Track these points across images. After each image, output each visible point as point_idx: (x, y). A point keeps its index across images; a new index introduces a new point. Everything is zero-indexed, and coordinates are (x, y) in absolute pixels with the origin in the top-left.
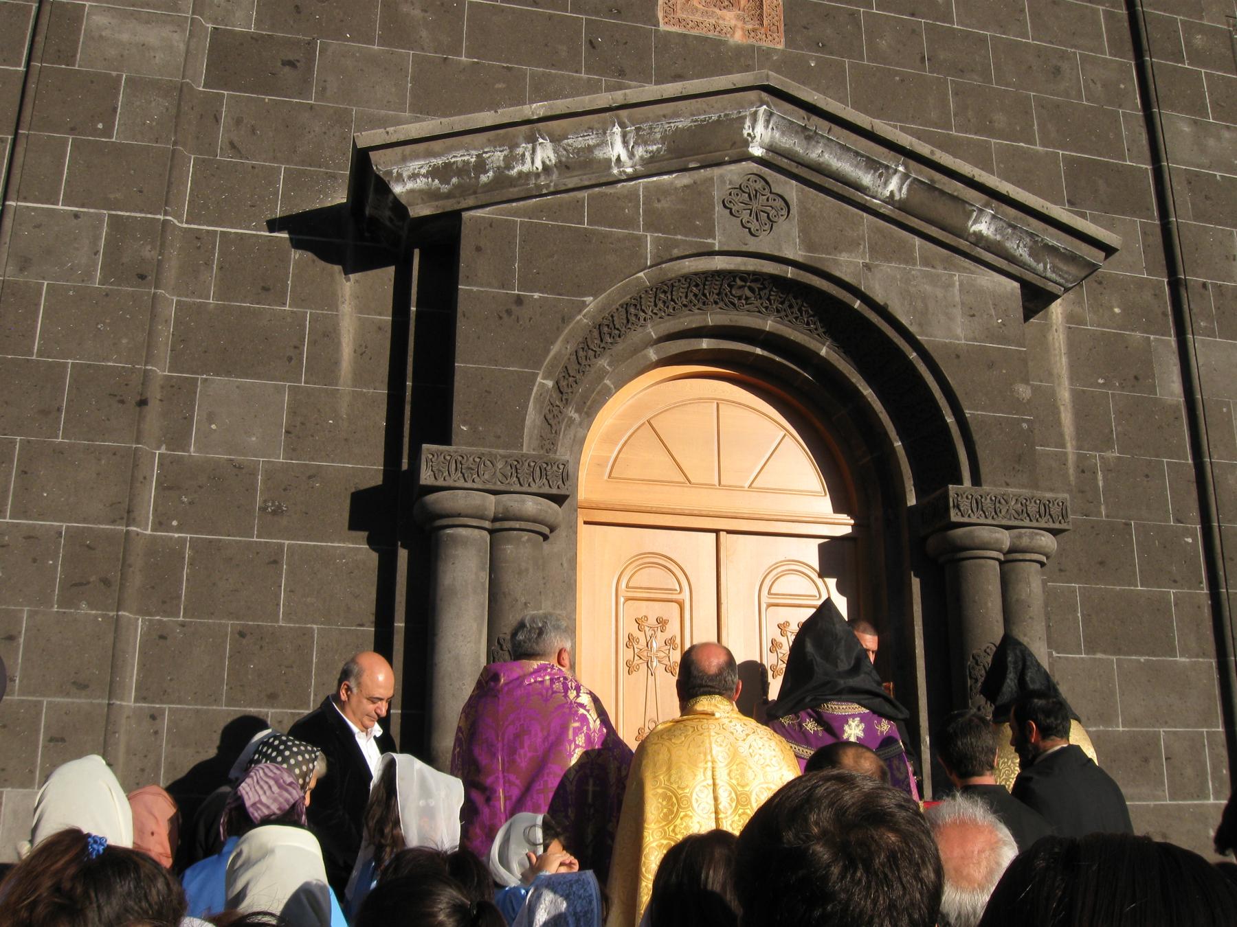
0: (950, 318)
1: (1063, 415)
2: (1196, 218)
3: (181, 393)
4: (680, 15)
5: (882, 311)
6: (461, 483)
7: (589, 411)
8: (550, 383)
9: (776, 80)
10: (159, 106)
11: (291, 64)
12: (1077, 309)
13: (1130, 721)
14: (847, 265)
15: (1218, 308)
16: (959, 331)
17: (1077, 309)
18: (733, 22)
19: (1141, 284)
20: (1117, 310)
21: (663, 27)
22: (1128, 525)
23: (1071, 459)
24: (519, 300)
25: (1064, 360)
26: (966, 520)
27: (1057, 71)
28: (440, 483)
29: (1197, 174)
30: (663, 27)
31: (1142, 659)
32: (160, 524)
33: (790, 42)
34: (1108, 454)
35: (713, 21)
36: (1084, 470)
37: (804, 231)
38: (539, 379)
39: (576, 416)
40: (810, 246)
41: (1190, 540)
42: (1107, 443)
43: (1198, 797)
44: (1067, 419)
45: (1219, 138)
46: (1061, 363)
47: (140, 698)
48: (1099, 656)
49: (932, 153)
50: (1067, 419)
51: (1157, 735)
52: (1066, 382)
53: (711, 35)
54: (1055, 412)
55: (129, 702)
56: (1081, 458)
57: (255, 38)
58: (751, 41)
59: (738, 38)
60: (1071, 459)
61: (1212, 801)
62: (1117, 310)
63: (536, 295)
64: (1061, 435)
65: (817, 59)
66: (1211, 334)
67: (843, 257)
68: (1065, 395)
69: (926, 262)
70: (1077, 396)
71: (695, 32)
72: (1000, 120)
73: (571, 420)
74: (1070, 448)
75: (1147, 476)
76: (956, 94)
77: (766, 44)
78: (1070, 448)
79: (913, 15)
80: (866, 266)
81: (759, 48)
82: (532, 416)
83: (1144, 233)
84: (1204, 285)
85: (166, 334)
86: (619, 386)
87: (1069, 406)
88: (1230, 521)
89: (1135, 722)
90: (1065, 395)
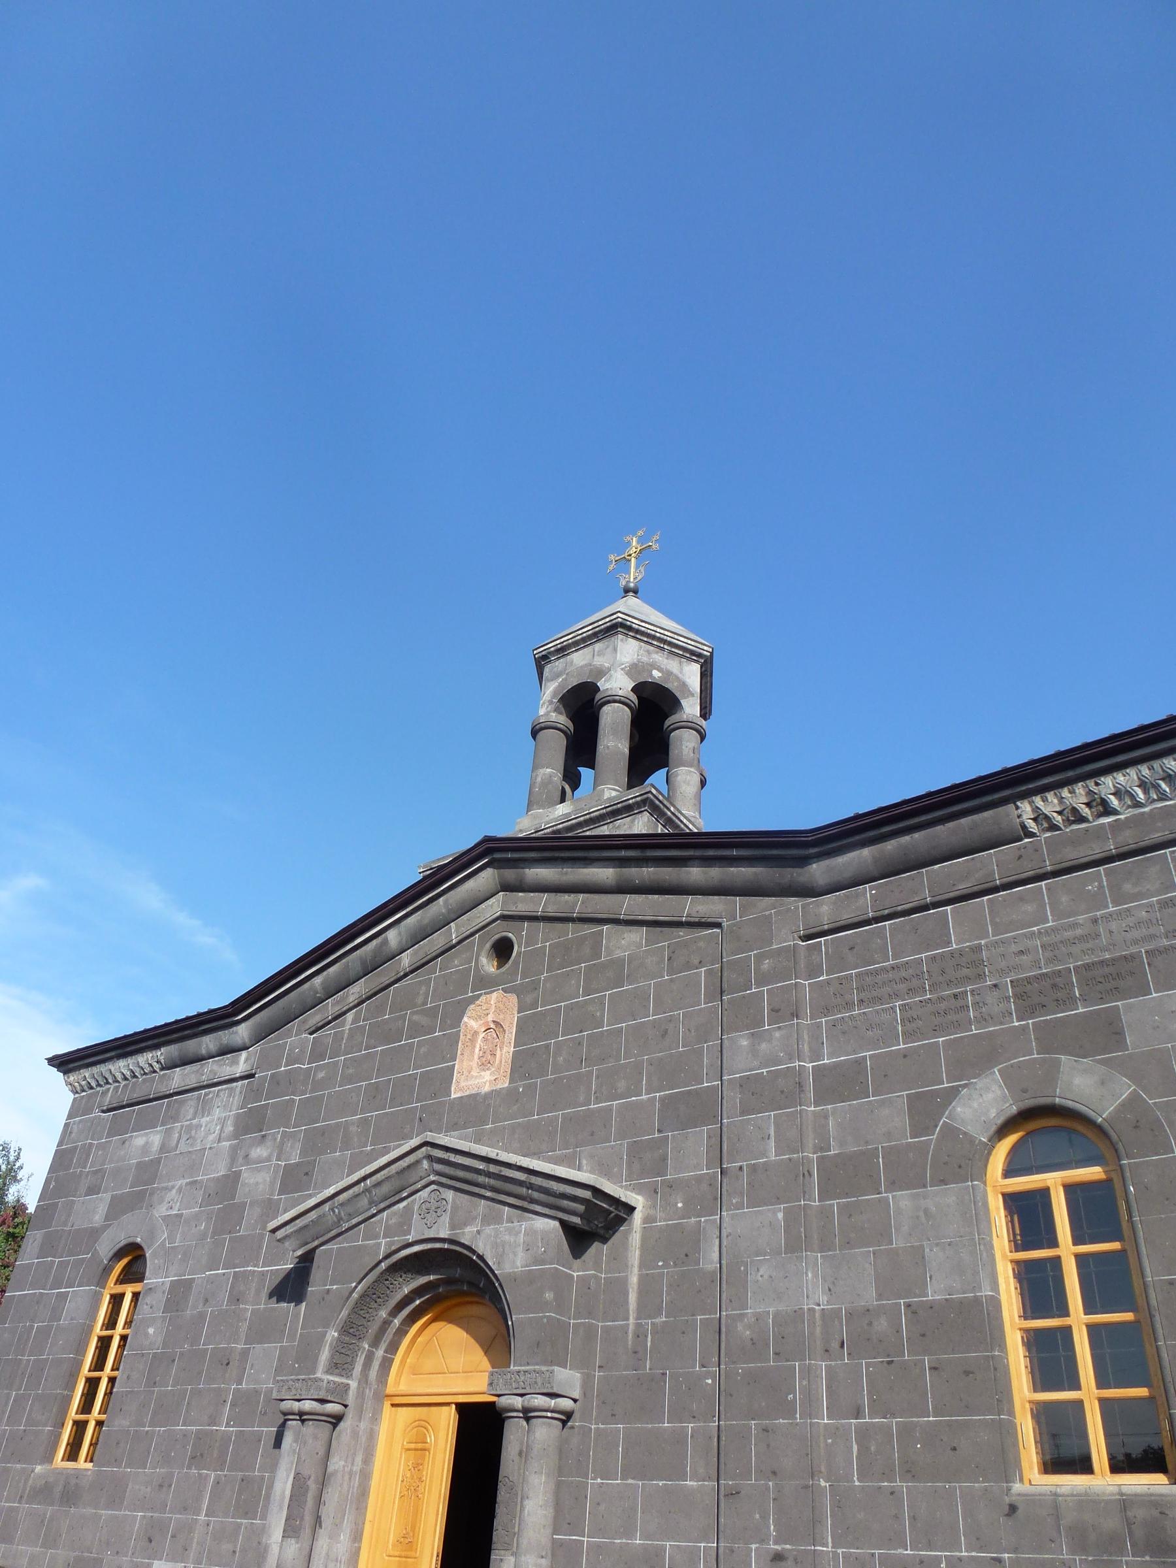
0: (515, 1254)
2: (743, 1113)
3: (245, 1353)
4: (463, 1084)
5: (481, 1257)
9: (430, 1136)
10: (257, 1210)
11: (307, 1174)
12: (652, 1212)
13: (644, 1537)
14: (467, 1235)
15: (749, 1184)
16: (519, 1264)
17: (652, 1212)
19: (699, 1179)
22: (664, 1374)
23: (631, 1327)
25: (637, 1252)
27: (666, 1032)
29: (748, 1077)
30: (453, 1096)
31: (661, 1483)
32: (228, 1425)
33: (512, 1081)
34: (657, 1320)
36: (640, 1335)
37: (451, 1219)
40: (453, 1227)
41: (710, 1381)
42: (659, 1313)
44: (633, 1298)
45: (770, 1041)
47: (206, 1515)
48: (630, 1481)
50: (633, 1298)
51: (663, 1548)
52: (636, 1270)
54: (626, 1294)
55: (202, 1517)
56: (638, 1326)
57: (297, 1164)
59: (487, 1089)
60: (631, 1327)
64: (628, 1311)
65: (524, 1086)
66: (740, 1206)
67: (468, 1229)
69: (510, 1221)
70: (642, 1279)
72: (622, 1085)
74: (632, 1320)
76: (597, 1077)
77: (499, 1086)
78: (632, 1320)
80: (478, 1232)
83: (709, 1137)
84: (741, 1168)
85: (244, 1326)
87: (636, 1287)
88: (734, 1363)
89: (648, 1538)
90: (634, 1280)
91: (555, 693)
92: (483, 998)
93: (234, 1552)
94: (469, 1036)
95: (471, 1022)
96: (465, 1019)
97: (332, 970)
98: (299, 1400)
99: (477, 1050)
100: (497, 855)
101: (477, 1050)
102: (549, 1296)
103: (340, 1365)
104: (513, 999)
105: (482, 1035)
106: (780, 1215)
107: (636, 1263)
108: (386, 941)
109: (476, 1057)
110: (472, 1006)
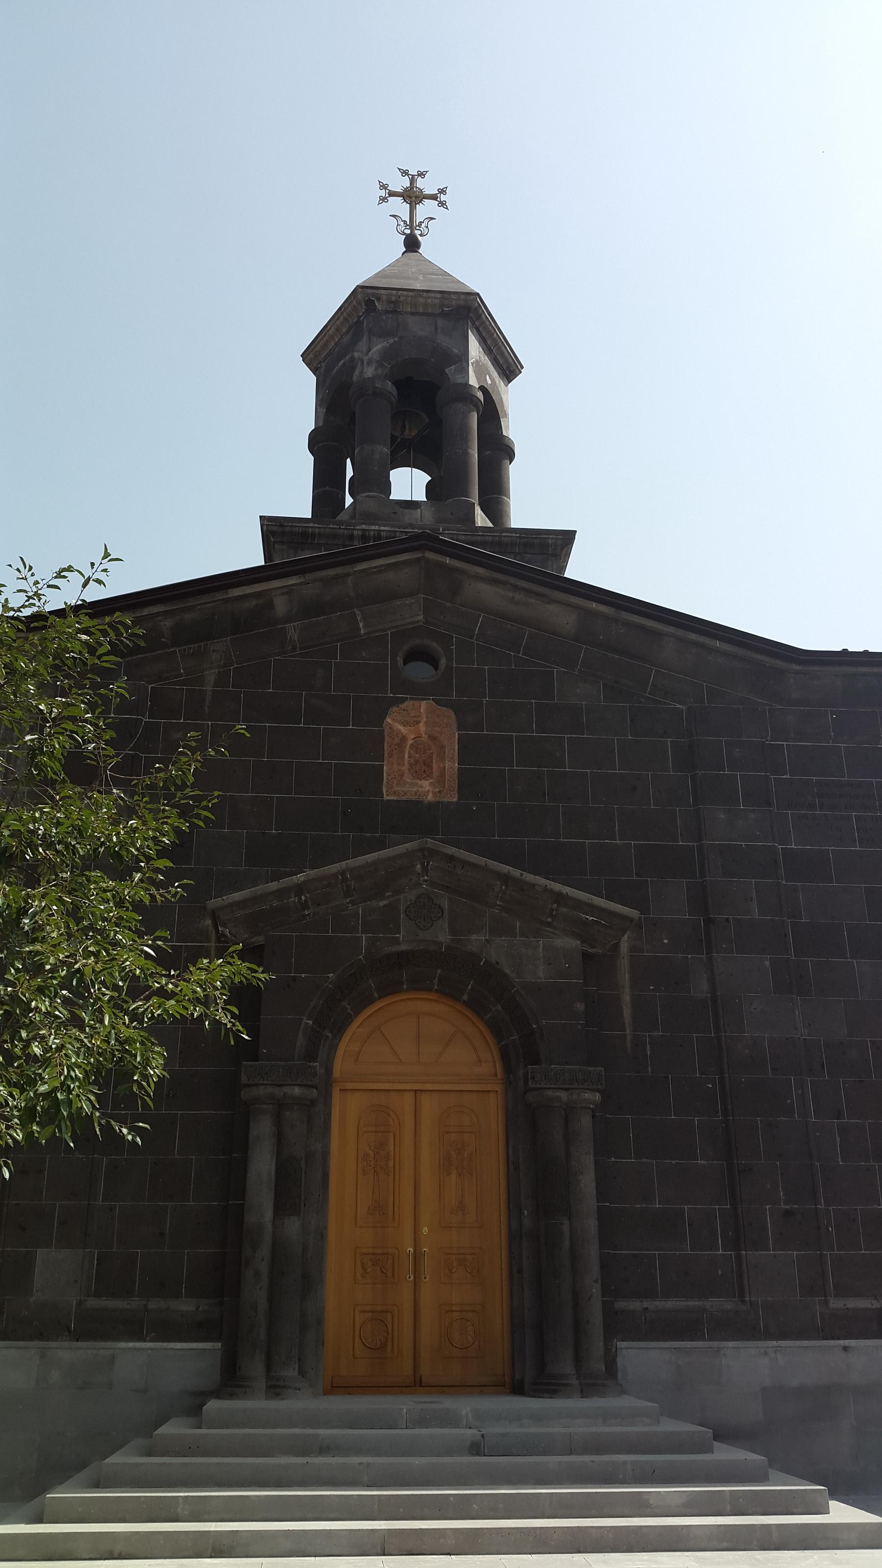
1: (625, 1011)
6: (261, 1082)
7: (340, 1030)
8: (311, 1022)
16: (541, 975)
18: (427, 788)
20: (665, 941)
21: (386, 798)
24: (294, 979)
25: (627, 976)
26: (538, 1086)
28: (251, 1082)
34: (655, 1034)
35: (415, 789)
38: (305, 1020)
39: (330, 1035)
43: (711, 1250)
44: (627, 1012)
46: (625, 978)
49: (522, 875)
50: (627, 1012)
52: (627, 990)
53: (413, 798)
58: (437, 799)
59: (430, 798)
61: (721, 1252)
62: (665, 941)
63: (303, 975)
67: (474, 937)
68: (627, 998)
71: (405, 798)
73: (327, 1037)
75: (681, 1046)
78: (628, 1031)
79: (539, 767)
80: (488, 941)
81: (442, 802)
82: (301, 1041)
84: (727, 920)
86: (358, 1011)
90: (627, 998)
91: (386, 354)
92: (408, 704)
93: (162, 1234)
94: (397, 740)
95: (394, 722)
96: (389, 720)
97: (188, 616)
98: (280, 1086)
99: (406, 756)
100: (430, 555)
101: (406, 756)
102: (580, 1006)
103: (311, 1055)
104: (449, 716)
105: (410, 742)
106: (767, 963)
107: (627, 984)
108: (270, 605)
109: (406, 762)
110: (395, 709)
